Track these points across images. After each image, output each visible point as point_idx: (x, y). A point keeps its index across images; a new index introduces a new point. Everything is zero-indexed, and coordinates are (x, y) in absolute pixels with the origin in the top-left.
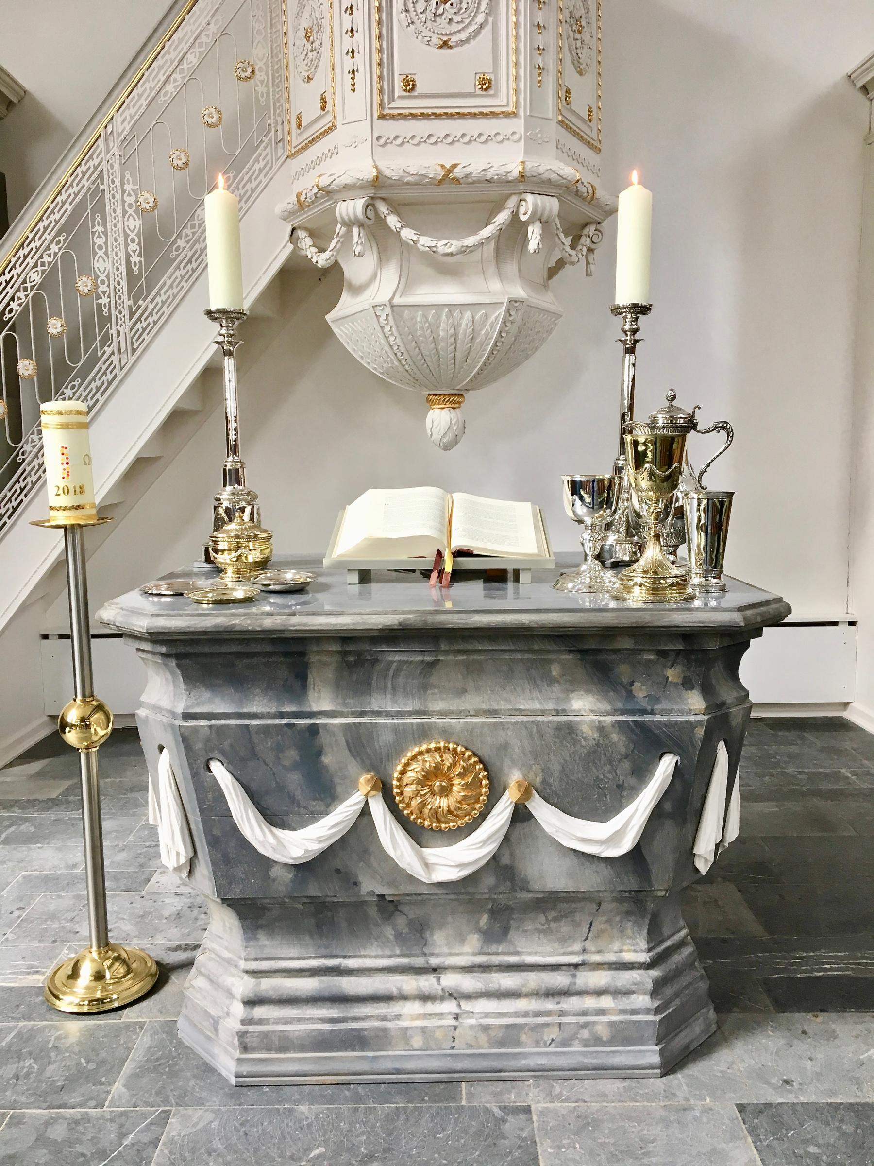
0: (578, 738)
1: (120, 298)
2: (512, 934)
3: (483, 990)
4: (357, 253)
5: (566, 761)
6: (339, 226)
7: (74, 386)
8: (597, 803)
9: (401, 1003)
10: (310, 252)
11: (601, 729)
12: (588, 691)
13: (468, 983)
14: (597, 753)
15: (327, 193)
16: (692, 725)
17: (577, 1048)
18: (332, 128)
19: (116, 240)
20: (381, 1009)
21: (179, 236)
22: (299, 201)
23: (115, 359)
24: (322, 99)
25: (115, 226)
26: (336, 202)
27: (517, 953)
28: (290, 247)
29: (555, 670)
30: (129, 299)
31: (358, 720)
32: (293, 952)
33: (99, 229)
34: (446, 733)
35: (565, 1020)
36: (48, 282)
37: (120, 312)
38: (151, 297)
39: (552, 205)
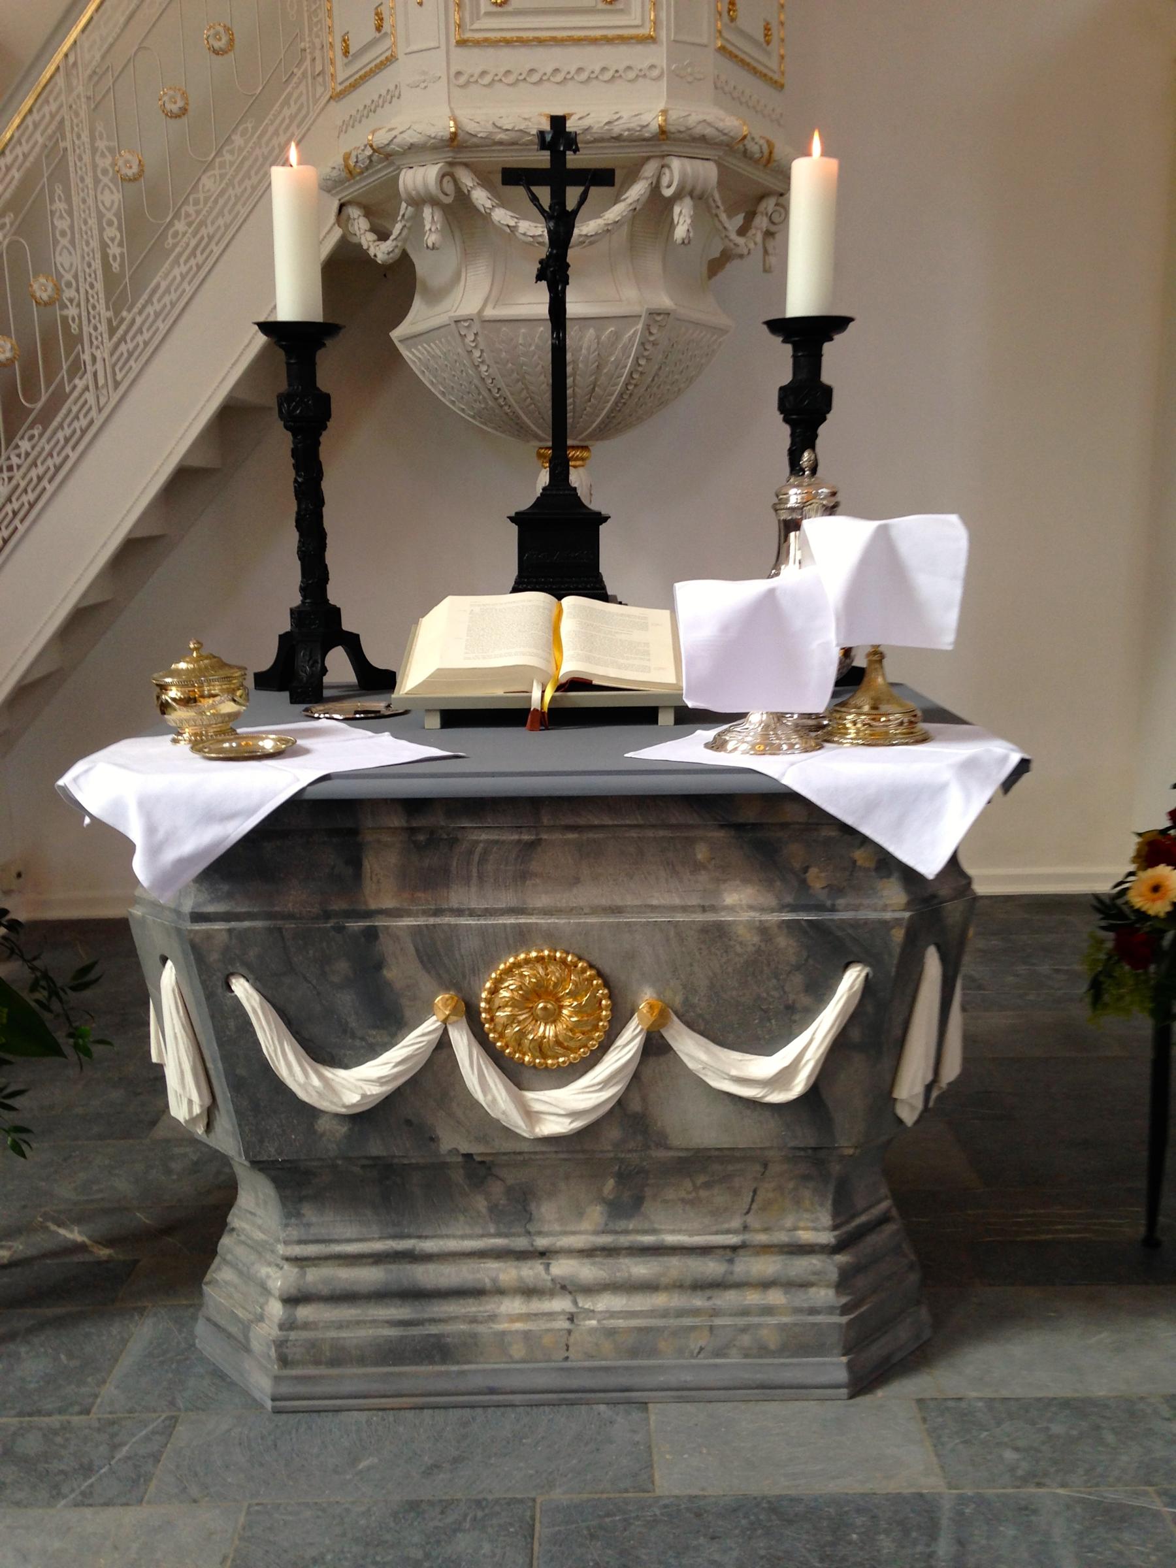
0: (732, 943)
1: (94, 307)
2: (648, 1207)
3: (608, 1281)
4: (430, 244)
5: (715, 974)
6: (404, 205)
7: (32, 437)
8: (761, 1030)
9: (496, 1299)
10: (367, 240)
11: (763, 930)
12: (746, 881)
13: (587, 1271)
14: (757, 964)
15: (388, 157)
16: (886, 925)
17: (734, 1359)
18: (391, 60)
19: (86, 223)
20: (470, 1307)
21: (177, 216)
22: (347, 166)
23: (90, 397)
24: (377, 14)
25: (84, 201)
26: (399, 169)
27: (653, 1231)
28: (338, 233)
29: (701, 853)
30: (108, 309)
31: (432, 921)
32: (350, 1231)
33: (61, 206)
34: (551, 937)
35: (718, 1321)
37: (96, 329)
38: (139, 305)
39: (707, 172)
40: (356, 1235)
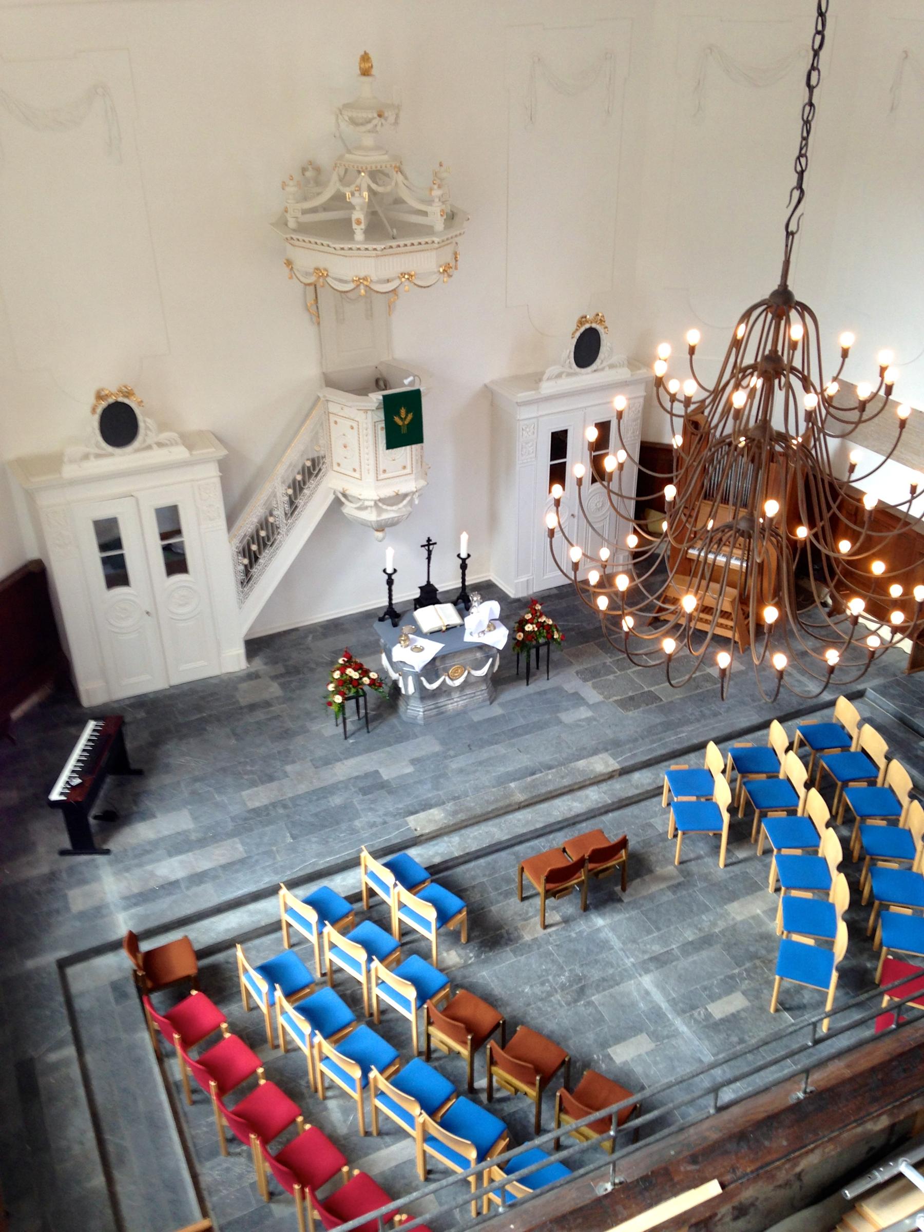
8: (479, 667)
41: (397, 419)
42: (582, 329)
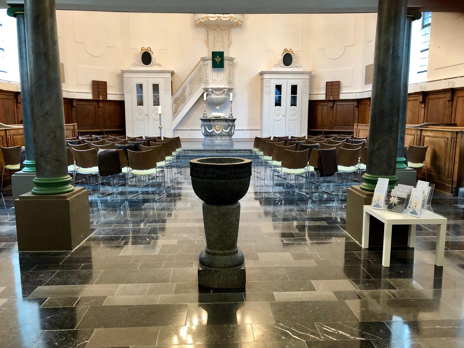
36: (181, 94)
40: (210, 138)
41: (216, 59)
42: (285, 53)
